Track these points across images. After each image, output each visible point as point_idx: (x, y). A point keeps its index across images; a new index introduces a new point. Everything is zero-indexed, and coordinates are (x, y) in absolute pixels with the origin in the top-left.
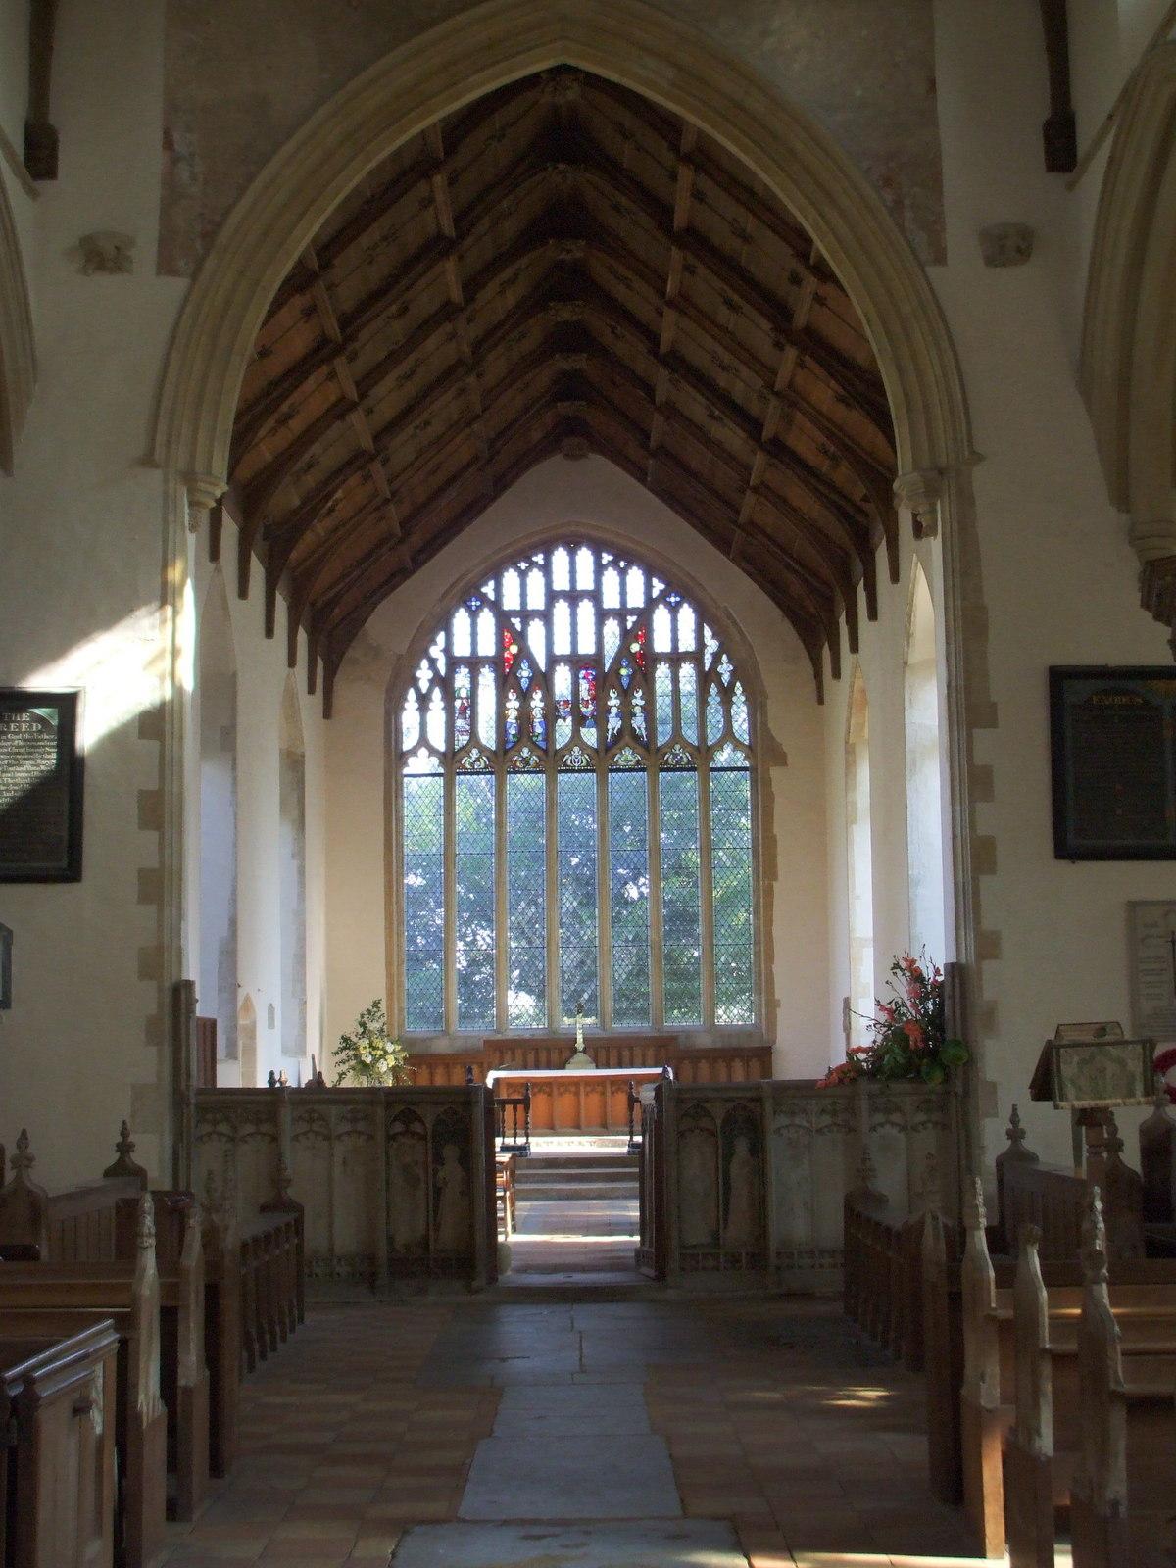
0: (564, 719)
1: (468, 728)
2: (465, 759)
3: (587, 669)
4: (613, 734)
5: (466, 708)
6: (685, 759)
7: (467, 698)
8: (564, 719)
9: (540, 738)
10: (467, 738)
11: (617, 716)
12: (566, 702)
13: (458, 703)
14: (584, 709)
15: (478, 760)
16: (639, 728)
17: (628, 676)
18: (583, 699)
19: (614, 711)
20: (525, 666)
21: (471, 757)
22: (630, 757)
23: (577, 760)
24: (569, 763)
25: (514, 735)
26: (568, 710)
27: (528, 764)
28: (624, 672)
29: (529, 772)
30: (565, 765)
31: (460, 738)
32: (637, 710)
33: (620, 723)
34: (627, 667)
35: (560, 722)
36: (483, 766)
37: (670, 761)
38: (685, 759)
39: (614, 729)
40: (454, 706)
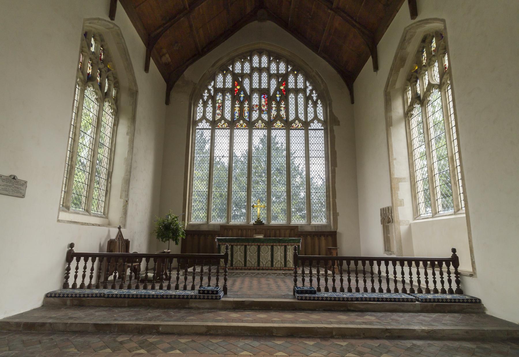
0: (256, 111)
1: (221, 113)
2: (219, 123)
3: (264, 95)
4: (273, 116)
5: (220, 106)
6: (300, 126)
7: (221, 103)
8: (256, 111)
9: (247, 117)
10: (220, 116)
11: (275, 110)
12: (257, 105)
13: (217, 105)
14: (263, 108)
15: (224, 124)
16: (283, 115)
17: (279, 97)
18: (263, 105)
19: (274, 109)
20: (242, 93)
21: (221, 123)
22: (280, 125)
23: (260, 125)
24: (257, 126)
25: (237, 116)
26: (257, 108)
27: (242, 126)
28: (278, 96)
29: (242, 129)
30: (256, 126)
31: (218, 116)
32: (282, 109)
33: (276, 113)
34: (279, 94)
35: (254, 112)
36: (225, 126)
37: (294, 126)
38: (300, 126)
39: (274, 115)
40: (216, 106)
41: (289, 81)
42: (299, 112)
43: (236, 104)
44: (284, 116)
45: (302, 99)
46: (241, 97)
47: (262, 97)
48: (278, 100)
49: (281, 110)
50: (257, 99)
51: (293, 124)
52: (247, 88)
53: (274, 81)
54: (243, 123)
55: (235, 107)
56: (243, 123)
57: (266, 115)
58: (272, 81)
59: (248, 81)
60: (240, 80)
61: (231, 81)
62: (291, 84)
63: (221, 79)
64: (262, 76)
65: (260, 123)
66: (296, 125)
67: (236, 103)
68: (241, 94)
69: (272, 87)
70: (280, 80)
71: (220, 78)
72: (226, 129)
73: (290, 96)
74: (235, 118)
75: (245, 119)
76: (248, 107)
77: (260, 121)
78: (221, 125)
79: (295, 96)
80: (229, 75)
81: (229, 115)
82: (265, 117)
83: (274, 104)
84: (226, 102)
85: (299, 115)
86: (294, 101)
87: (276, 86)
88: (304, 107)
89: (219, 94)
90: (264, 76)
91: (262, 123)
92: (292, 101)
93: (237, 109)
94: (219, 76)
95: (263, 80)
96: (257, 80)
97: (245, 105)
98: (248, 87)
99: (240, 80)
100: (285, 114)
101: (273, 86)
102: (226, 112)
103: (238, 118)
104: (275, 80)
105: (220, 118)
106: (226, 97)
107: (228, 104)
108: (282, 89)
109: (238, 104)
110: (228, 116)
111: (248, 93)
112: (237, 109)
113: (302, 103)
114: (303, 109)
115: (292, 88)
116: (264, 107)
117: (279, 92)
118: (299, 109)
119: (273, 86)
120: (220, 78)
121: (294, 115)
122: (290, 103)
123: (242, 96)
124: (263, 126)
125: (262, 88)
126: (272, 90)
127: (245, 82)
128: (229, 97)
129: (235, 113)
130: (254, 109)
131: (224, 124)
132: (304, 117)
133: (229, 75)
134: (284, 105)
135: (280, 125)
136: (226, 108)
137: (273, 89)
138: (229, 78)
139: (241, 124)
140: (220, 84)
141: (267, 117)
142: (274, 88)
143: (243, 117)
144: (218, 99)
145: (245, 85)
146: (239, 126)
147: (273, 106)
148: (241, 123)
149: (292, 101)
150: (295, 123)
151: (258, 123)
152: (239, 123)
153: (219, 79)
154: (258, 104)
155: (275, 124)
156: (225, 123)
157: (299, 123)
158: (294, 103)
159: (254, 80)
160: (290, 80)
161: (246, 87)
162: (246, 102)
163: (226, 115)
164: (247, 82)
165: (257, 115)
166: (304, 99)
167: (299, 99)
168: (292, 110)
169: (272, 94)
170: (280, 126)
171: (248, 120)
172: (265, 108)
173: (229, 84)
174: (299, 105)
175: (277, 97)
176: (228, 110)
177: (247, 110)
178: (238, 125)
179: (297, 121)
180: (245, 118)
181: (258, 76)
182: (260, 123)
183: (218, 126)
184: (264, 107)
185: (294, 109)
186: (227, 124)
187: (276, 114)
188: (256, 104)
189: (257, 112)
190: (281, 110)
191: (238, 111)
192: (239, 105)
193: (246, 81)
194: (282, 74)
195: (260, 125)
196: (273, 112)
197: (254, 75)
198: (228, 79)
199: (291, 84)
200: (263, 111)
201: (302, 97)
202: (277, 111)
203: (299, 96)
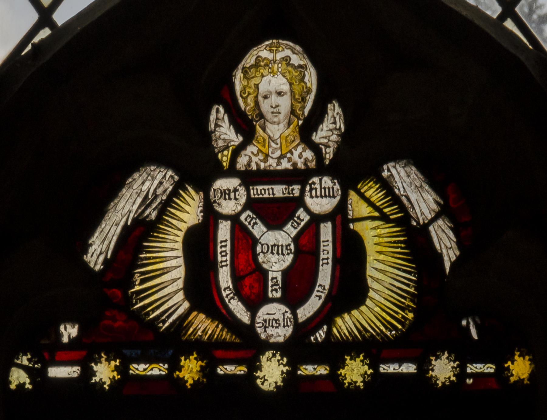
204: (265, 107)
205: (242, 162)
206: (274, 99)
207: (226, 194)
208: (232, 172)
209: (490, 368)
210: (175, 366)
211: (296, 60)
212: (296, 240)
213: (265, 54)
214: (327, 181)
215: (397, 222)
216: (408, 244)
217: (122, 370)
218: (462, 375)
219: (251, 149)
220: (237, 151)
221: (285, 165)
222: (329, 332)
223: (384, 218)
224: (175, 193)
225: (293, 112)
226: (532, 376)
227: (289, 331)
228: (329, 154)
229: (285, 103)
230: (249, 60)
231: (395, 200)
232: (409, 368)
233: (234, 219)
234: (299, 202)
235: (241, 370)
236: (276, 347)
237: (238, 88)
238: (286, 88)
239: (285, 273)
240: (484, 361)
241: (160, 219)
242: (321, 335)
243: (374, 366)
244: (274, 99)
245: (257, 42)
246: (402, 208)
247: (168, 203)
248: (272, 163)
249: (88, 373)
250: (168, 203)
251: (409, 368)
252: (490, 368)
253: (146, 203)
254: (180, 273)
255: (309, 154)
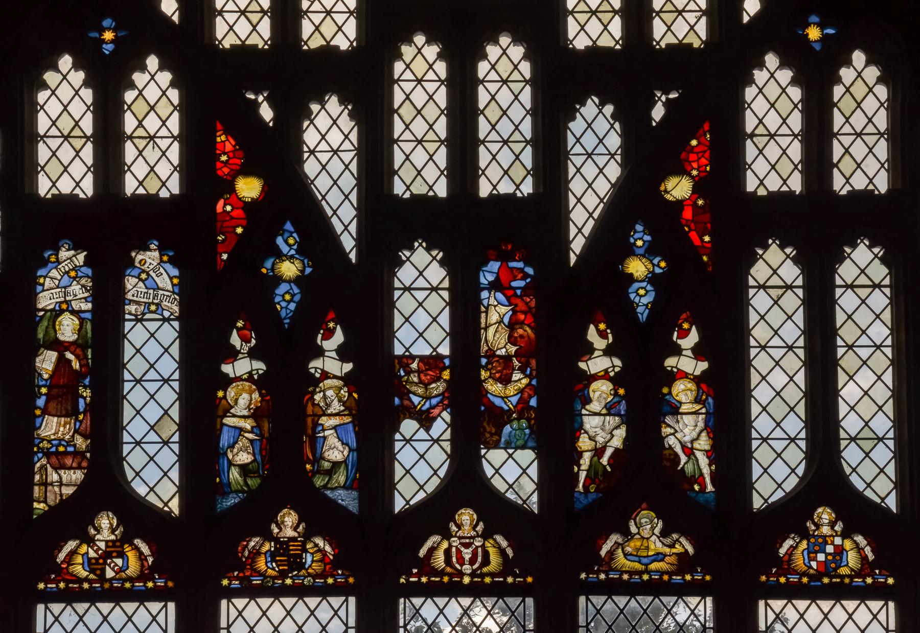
0: (426, 420)
2: (71, 545)
3: (504, 258)
4: (593, 468)
5: (78, 376)
6: (852, 559)
8: (426, 420)
10: (77, 476)
11: (610, 409)
12: (432, 362)
13: (46, 362)
14: (494, 387)
15: (115, 549)
16: (689, 452)
17: (653, 279)
18: (491, 354)
19: (601, 391)
20: (286, 243)
22: (656, 545)
23: (467, 554)
24: (439, 560)
26: (438, 388)
27: (296, 564)
28: (637, 267)
29: (300, 592)
30: (426, 565)
32: (683, 392)
33: (621, 433)
34: (650, 252)
35: (409, 426)
36: (133, 568)
37: (799, 561)
38: (852, 559)
39: (599, 452)
40: (33, 371)
41: (750, 123)
42: (850, 424)
43: (232, 355)
44: (703, 461)
45: (880, 300)
46: (278, 280)
47: (487, 277)
48: (643, 313)
49: (675, 410)
50: (438, 303)
51: (788, 543)
52: (334, 198)
53: (602, 125)
54: (308, 536)
55: (226, 382)
56: (308, 536)
57: (527, 456)
58: (577, 126)
59: (346, 123)
60: (267, 113)
61: (174, 124)
62: (773, 152)
63: (77, 108)
64: (483, 68)
65: (467, 531)
66: (811, 553)
67: (235, 340)
68: (279, 255)
69: (577, 186)
70: (658, 113)
71: (65, 92)
72: (142, 597)
73: (759, 272)
74: (225, 489)
75: (318, 494)
76: (347, 379)
77: (466, 516)
78: (91, 564)
79: (806, 272)
80: (152, 62)
81: (169, 457)
82: (511, 472)
83: (600, 344)
84: (135, 334)
85: (851, 455)
86: (799, 318)
87: (614, 171)
88: (897, 377)
89: (64, 254)
90: (504, 68)
91: (486, 535)
92: (776, 317)
93: (243, 400)
94: (50, 77)
95: (493, 113)
96: (431, 112)
97: (315, 365)
98: (348, 182)
99: (267, 113)
100: (704, 443)
101: (590, 170)
102: (135, 428)
103: (253, 482)
104: (609, 109)
105: (82, 487)
106: (130, 282)
107: (152, 351)
108: (679, 204)
109: (253, 354)
110: (152, 474)
111: (348, 243)
112: (243, 400)
113: (881, 332)
114: (882, 393)
115: (774, 197)
116: (506, 380)
117: (648, 229)
118: (849, 392)
119: (590, 170)
120: (65, 92)
121: (796, 455)
122: (760, 333)
123: (289, 269)
124: (495, 560)
125: (485, 190)
126: (578, 216)
127: (310, 137)
128: (164, 282)
129: (225, 440)
130: (405, 394)
131: (115, 549)
132: (891, 470)
133: (152, 62)
134: (698, 352)
135: (656, 545)
136: (135, 396)
137: (591, 201)
138: (152, 93)
139: (282, 546)
140: (66, 153)
141: (533, 471)
142: (603, 187)
143: (308, 479)
144: (46, 301)
145: (310, 168)
146: (261, 564)
147: (597, 364)
148: (289, 533)
149: (776, 317)
150: (804, 534)
151: (447, 535)
152: (268, 536)
153: (54, 107)
154: (445, 350)
155: (615, 538)
156: (127, 539)
157: (845, 535)
158: (792, 332)
159: (407, 112)
160: (760, 106)
161: (322, 184)
162: (329, 334)
163: (134, 459)
164: (335, 138)
165: (439, 457)
166: (894, 301)
167: (847, 301)
168: (777, 409)
169: (577, 245)
170: (660, 557)
171: (348, 500)
172: (511, 390)
173: (152, 155)
174: (848, 361)
175: (631, 279)
176: (152, 413)
177: (336, 407)
178: (256, 553)
179: (825, 514)
180: (319, 482)
181: (441, 68)
182: (467, 531)
183: (57, 569)
184: (506, 380)
185: (794, 395)
186: (145, 549)
187: (617, 442)
188: (422, 350)
189: (440, 427)
190: (675, 410)
191: (247, 425)
192: (260, 366)
193: (322, 121)
194: (681, 50)
195: (467, 554)
196: (591, 423)
197: (398, 67)
198: (140, 108)
199: (773, 152)
200: (500, 417)
201: (879, 272)
202: (628, 420)
203: (846, 272)
204: (464, 523)
205: (458, 534)
206: (466, 521)
207: (454, 541)
208: (455, 536)
209: (522, 580)
210: (442, 578)
211: (471, 513)
212: (472, 551)
213: (463, 511)
214: (480, 539)
215: (497, 548)
216: (500, 552)
217: (429, 579)
218: (515, 581)
219: (460, 532)
220: (457, 532)
221: (469, 535)
222: (481, 571)
223: (494, 547)
224: (441, 541)
225: (471, 524)
226: (533, 581)
227: (471, 571)
228: (480, 533)
229: (469, 522)
230: (459, 512)
231: (497, 543)
232: (501, 579)
233: (456, 547)
234: (473, 543)
235: (459, 579)
236: (468, 575)
237: (457, 519)
238: (469, 518)
239: (470, 559)
240: (520, 578)
241: (437, 547)
242: (479, 572)
243: (493, 579)
244: (466, 521)
245: (461, 508)
246: (499, 544)
247: (440, 543)
248: (466, 535)
249: (420, 580)
250: (440, 543)
251: (501, 579)
252: (522, 580)
253: (434, 543)
254: (443, 558)
255: (475, 533)
